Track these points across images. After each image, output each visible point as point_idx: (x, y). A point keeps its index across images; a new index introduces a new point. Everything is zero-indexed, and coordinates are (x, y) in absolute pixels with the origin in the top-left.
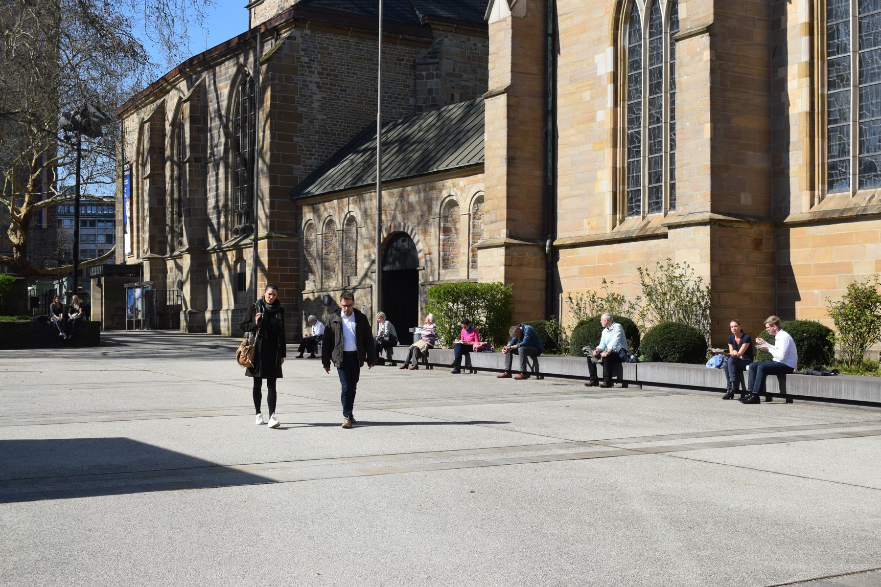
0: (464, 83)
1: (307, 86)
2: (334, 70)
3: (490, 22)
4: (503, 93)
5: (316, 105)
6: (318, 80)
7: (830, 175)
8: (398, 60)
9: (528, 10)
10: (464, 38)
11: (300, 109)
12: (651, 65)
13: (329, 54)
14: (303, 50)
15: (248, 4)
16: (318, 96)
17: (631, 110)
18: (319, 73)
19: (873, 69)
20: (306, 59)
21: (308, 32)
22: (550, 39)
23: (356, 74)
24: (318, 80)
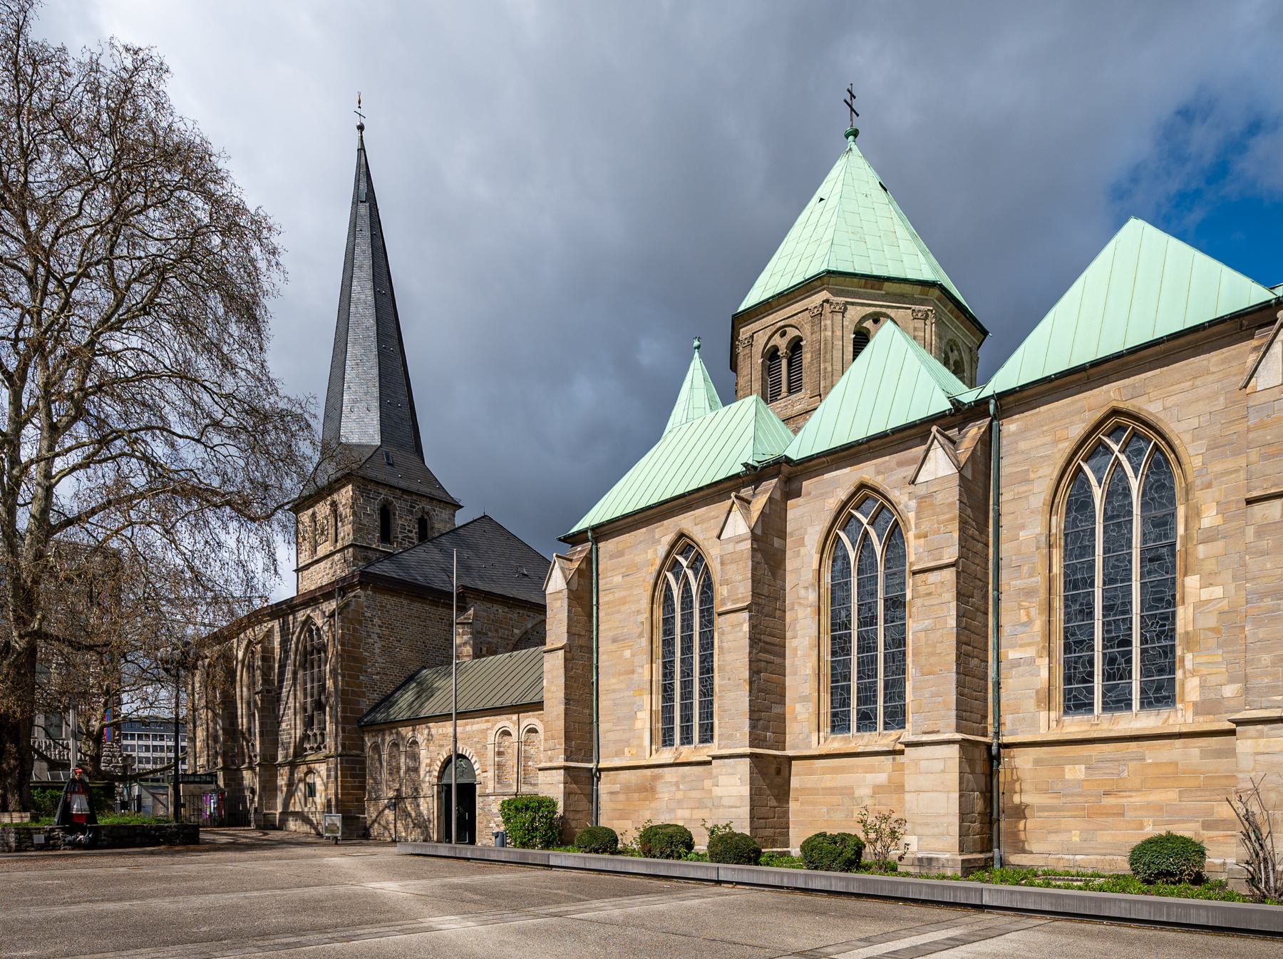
0: (490, 640)
2: (391, 625)
4: (561, 649)
5: (377, 651)
7: (833, 721)
8: (441, 619)
10: (489, 605)
12: (682, 632)
15: (295, 568)
18: (379, 626)
19: (870, 643)
21: (371, 593)
24: (379, 631)
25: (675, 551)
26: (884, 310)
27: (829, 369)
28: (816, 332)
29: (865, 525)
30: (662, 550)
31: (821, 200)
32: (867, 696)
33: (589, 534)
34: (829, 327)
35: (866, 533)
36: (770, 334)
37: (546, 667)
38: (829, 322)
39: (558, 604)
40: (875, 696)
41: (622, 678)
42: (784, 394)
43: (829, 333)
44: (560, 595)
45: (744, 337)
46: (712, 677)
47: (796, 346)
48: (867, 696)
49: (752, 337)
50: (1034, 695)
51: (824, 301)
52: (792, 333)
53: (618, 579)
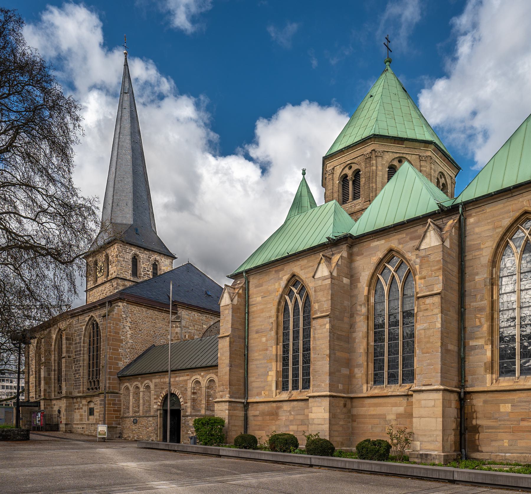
1: (125, 327)
2: (136, 322)
3: (221, 305)
5: (129, 336)
6: (130, 325)
7: (375, 378)
8: (163, 319)
9: (238, 301)
10: (190, 312)
11: (122, 337)
12: (294, 328)
13: (134, 314)
14: (123, 312)
16: (130, 332)
17: (284, 346)
20: (124, 316)
21: (126, 304)
22: (247, 314)
23: (146, 324)
24: (130, 325)
25: (290, 284)
26: (404, 156)
27: (374, 187)
28: (368, 167)
29: (393, 271)
30: (283, 283)
31: (371, 96)
32: (393, 364)
33: (244, 274)
34: (375, 165)
35: (393, 277)
36: (343, 168)
37: (220, 346)
38: (374, 162)
39: (227, 312)
40: (398, 365)
41: (261, 353)
42: (350, 200)
43: (374, 168)
44: (228, 307)
45: (329, 169)
46: (310, 353)
47: (357, 173)
48: (393, 364)
49: (333, 169)
50: (483, 365)
51: (372, 150)
52: (355, 167)
53: (259, 299)
